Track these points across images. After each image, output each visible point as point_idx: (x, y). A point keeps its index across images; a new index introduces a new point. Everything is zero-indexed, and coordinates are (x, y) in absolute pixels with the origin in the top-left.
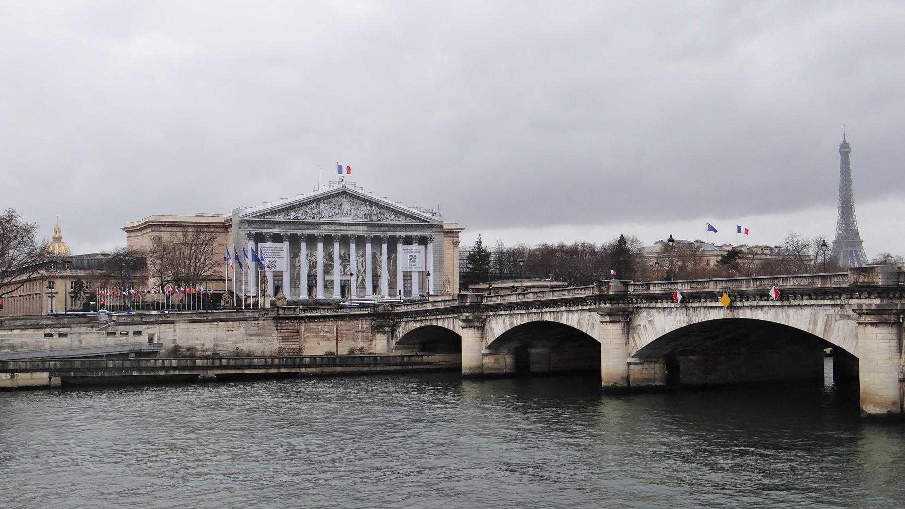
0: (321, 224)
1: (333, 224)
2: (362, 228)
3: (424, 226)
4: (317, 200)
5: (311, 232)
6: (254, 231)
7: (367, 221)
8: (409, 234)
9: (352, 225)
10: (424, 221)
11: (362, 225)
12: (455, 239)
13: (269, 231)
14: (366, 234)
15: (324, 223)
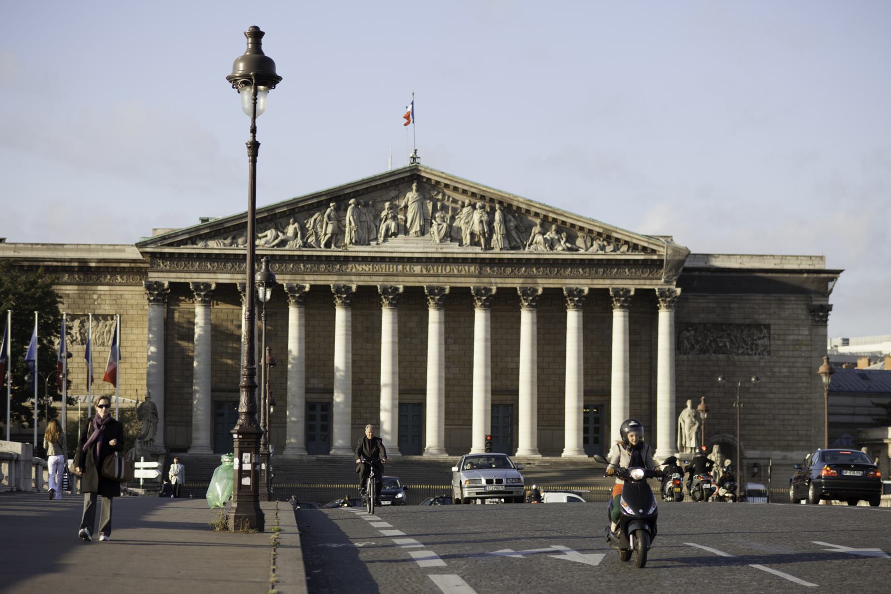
0: (346, 260)
1: (382, 260)
2: (465, 269)
3: (645, 264)
4: (337, 198)
5: (321, 280)
6: (165, 278)
7: (478, 252)
8: (601, 283)
9: (437, 261)
10: (645, 249)
11: (465, 261)
12: (817, 302)
13: (203, 278)
14: (471, 283)
15: (356, 259)
